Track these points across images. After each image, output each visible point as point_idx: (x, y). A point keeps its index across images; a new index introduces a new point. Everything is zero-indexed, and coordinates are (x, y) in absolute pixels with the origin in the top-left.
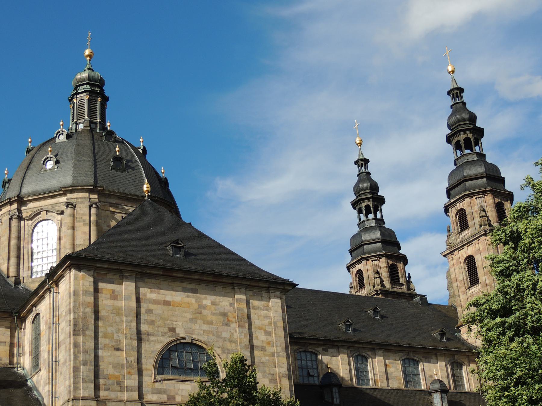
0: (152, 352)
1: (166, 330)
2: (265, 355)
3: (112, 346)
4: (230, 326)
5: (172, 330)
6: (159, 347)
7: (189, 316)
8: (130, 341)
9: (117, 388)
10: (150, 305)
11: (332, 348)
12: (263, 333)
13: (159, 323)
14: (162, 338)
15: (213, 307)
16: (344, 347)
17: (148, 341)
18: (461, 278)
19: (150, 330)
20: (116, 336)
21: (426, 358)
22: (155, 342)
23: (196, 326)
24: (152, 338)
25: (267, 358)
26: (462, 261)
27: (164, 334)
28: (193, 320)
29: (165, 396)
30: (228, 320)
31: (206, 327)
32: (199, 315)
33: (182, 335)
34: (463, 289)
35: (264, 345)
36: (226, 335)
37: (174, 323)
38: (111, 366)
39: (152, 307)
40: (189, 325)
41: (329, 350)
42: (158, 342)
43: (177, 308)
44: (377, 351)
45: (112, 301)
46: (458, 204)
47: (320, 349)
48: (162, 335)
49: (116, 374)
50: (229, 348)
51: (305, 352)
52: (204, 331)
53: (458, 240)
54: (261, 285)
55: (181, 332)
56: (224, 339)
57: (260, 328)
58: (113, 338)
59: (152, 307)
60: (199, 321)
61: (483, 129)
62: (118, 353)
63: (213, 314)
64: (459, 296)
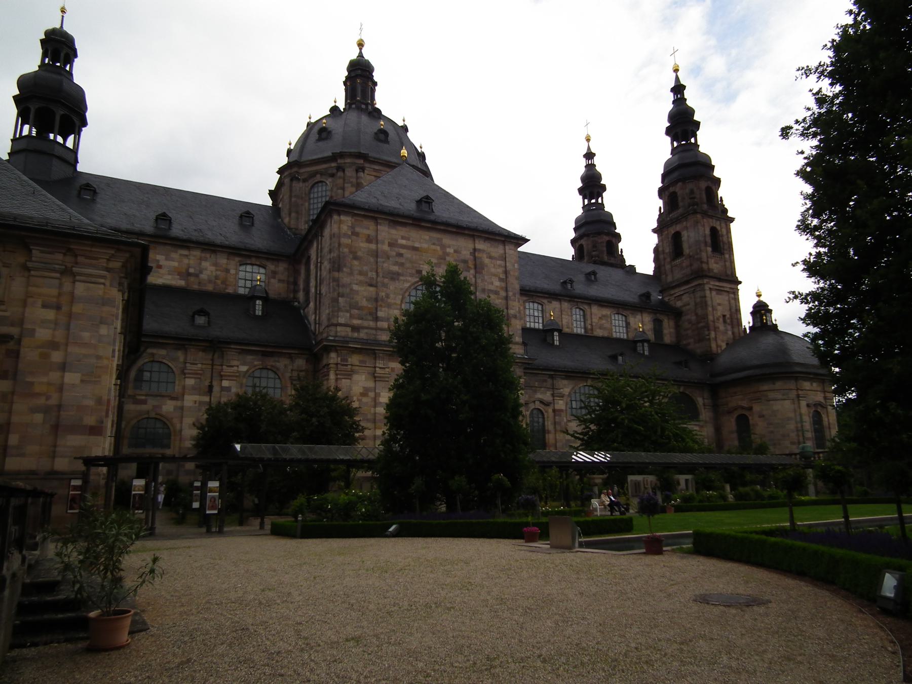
0: (401, 289)
1: (414, 271)
2: (498, 298)
3: (366, 282)
4: (469, 271)
5: (420, 272)
8: (382, 279)
9: (370, 318)
10: (401, 250)
13: (408, 265)
14: (410, 279)
15: (455, 254)
16: (565, 301)
17: (398, 279)
18: (667, 251)
19: (400, 271)
20: (370, 274)
21: (632, 314)
22: (404, 281)
24: (401, 278)
25: (500, 301)
26: (670, 236)
27: (412, 275)
30: (470, 268)
34: (668, 260)
35: (499, 290)
37: (421, 266)
38: (365, 299)
39: (402, 251)
41: (553, 302)
42: (407, 281)
43: (424, 254)
44: (592, 306)
45: (368, 244)
46: (671, 188)
47: (545, 301)
48: (410, 276)
49: (369, 306)
51: (533, 302)
53: (668, 219)
54: (497, 238)
57: (495, 275)
58: (367, 275)
59: (402, 251)
61: (700, 122)
62: (371, 289)
64: (664, 265)
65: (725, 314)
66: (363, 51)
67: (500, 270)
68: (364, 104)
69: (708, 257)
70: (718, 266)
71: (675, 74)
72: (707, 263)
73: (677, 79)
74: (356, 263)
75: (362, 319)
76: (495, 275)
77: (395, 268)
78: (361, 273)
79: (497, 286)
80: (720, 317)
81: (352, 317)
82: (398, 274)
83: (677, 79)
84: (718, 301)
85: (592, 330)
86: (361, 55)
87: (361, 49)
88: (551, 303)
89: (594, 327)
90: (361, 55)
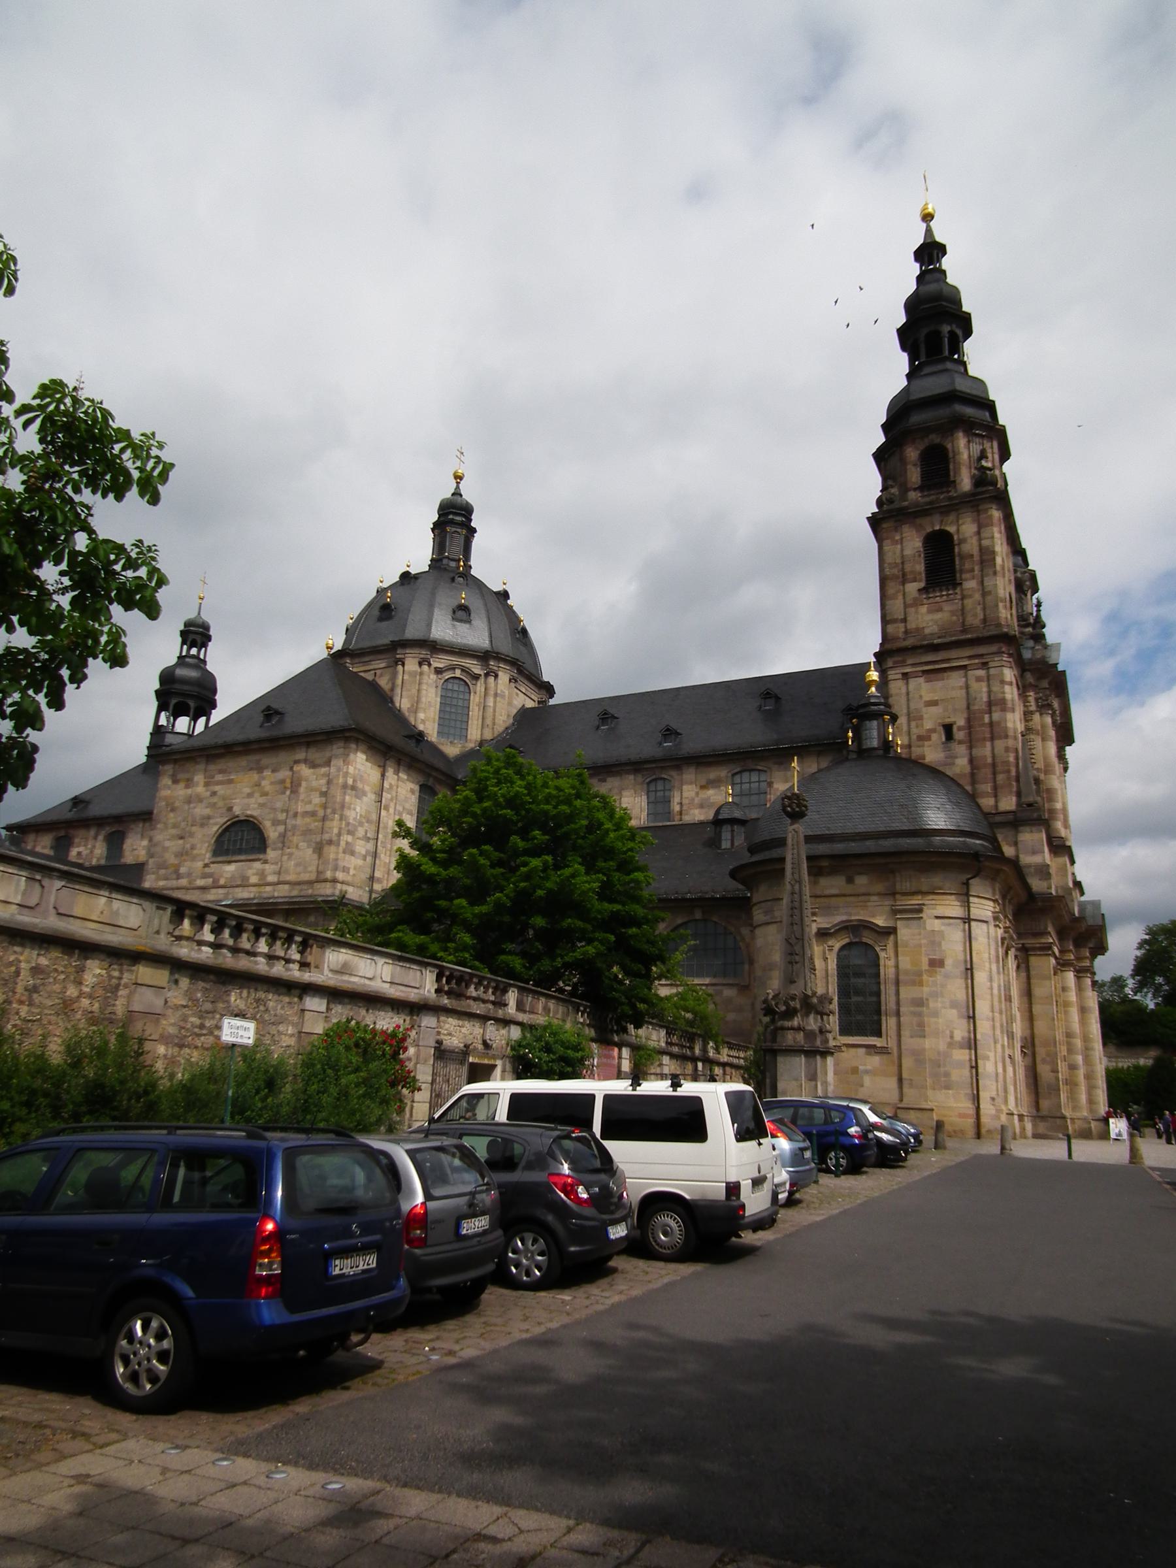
1: (224, 810)
2: (315, 821)
4: (285, 793)
5: (230, 809)
6: (215, 828)
7: (247, 790)
11: (613, 776)
12: (318, 795)
16: (628, 772)
23: (252, 800)
24: (211, 821)
28: (250, 795)
29: (211, 880)
31: (261, 800)
32: (256, 788)
33: (237, 813)
36: (279, 805)
39: (217, 788)
40: (246, 801)
42: (216, 824)
50: (280, 818)
52: (262, 805)
55: (237, 810)
56: (275, 810)
57: (316, 790)
60: (257, 795)
63: (272, 783)
65: (947, 721)
66: (461, 486)
67: (323, 781)
68: (453, 560)
69: (906, 606)
70: (938, 616)
71: (924, 225)
72: (904, 620)
73: (929, 231)
74: (172, 815)
75: (167, 879)
76: (316, 790)
77: (207, 811)
78: (175, 826)
79: (316, 805)
80: (933, 731)
81: (158, 879)
82: (209, 818)
83: (929, 231)
84: (927, 697)
85: (681, 813)
86: (457, 493)
87: (458, 483)
88: (605, 781)
89: (685, 808)
90: (457, 493)
